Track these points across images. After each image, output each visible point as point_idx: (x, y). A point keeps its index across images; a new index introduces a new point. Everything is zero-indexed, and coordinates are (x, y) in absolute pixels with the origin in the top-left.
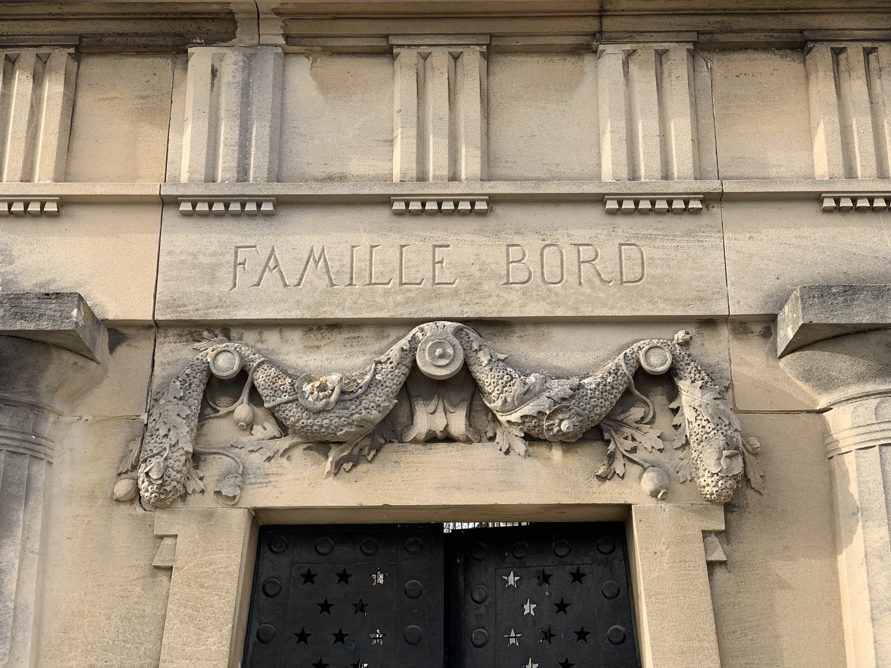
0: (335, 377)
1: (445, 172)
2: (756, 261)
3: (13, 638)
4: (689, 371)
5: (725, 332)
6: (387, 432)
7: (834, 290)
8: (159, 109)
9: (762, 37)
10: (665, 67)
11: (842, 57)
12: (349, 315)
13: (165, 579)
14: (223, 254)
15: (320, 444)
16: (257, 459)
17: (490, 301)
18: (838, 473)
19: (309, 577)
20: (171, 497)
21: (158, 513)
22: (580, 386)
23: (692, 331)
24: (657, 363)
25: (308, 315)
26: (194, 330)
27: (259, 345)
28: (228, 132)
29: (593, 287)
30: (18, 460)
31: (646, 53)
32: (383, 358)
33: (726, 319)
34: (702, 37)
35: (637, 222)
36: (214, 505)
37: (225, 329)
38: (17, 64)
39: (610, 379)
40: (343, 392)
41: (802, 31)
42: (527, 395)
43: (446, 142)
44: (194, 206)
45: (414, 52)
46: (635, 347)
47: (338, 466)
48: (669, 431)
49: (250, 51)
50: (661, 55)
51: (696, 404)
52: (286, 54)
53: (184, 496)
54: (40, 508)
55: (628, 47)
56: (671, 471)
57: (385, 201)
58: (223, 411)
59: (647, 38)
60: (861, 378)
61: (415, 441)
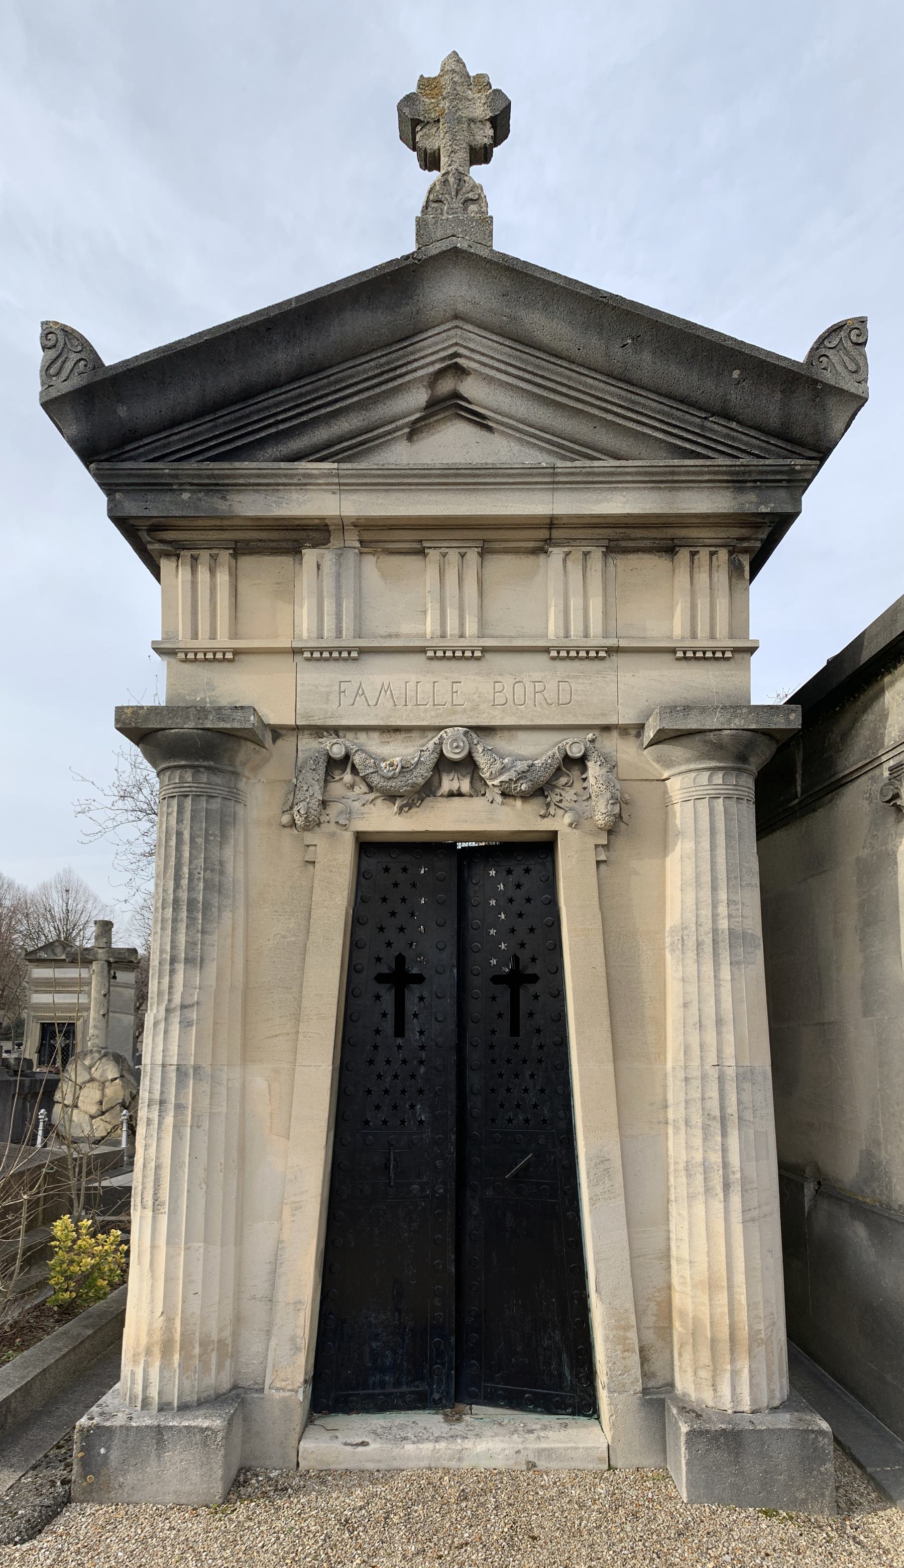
0: (398, 759)
1: (457, 632)
2: (636, 690)
3: (234, 897)
4: (593, 757)
5: (615, 734)
6: (426, 791)
7: (678, 709)
8: (286, 591)
9: (648, 543)
10: (588, 563)
11: (696, 557)
12: (405, 723)
13: (312, 868)
14: (332, 686)
15: (391, 797)
16: (357, 805)
17: (484, 716)
18: (670, 814)
19: (387, 870)
20: (312, 824)
21: (306, 833)
22: (533, 765)
23: (597, 733)
24: (576, 752)
25: (382, 723)
26: (319, 731)
27: (355, 741)
28: (329, 606)
29: (542, 708)
30: (228, 802)
31: (577, 554)
32: (424, 748)
33: (616, 727)
34: (612, 543)
35: (568, 664)
36: (335, 829)
37: (336, 730)
38: (199, 561)
39: (549, 761)
40: (403, 767)
41: (673, 539)
42: (504, 769)
43: (457, 612)
44: (312, 654)
45: (437, 552)
46: (564, 743)
47: (401, 809)
48: (580, 791)
49: (339, 552)
50: (586, 554)
51: (596, 775)
52: (361, 553)
53: (319, 824)
54: (242, 829)
55: (566, 549)
56: (581, 812)
57: (422, 650)
58: (337, 778)
59: (578, 543)
60: (688, 761)
61: (442, 796)
